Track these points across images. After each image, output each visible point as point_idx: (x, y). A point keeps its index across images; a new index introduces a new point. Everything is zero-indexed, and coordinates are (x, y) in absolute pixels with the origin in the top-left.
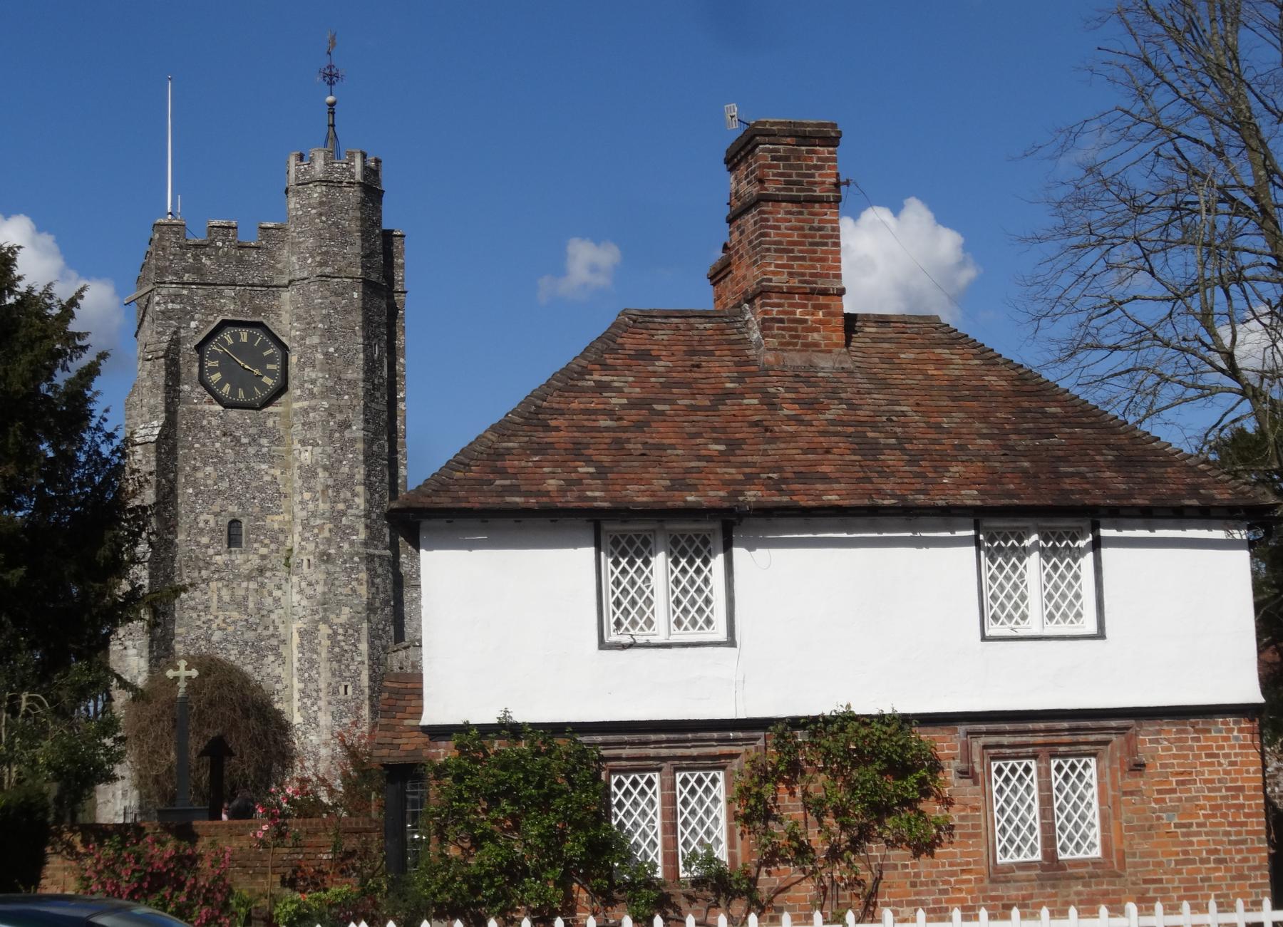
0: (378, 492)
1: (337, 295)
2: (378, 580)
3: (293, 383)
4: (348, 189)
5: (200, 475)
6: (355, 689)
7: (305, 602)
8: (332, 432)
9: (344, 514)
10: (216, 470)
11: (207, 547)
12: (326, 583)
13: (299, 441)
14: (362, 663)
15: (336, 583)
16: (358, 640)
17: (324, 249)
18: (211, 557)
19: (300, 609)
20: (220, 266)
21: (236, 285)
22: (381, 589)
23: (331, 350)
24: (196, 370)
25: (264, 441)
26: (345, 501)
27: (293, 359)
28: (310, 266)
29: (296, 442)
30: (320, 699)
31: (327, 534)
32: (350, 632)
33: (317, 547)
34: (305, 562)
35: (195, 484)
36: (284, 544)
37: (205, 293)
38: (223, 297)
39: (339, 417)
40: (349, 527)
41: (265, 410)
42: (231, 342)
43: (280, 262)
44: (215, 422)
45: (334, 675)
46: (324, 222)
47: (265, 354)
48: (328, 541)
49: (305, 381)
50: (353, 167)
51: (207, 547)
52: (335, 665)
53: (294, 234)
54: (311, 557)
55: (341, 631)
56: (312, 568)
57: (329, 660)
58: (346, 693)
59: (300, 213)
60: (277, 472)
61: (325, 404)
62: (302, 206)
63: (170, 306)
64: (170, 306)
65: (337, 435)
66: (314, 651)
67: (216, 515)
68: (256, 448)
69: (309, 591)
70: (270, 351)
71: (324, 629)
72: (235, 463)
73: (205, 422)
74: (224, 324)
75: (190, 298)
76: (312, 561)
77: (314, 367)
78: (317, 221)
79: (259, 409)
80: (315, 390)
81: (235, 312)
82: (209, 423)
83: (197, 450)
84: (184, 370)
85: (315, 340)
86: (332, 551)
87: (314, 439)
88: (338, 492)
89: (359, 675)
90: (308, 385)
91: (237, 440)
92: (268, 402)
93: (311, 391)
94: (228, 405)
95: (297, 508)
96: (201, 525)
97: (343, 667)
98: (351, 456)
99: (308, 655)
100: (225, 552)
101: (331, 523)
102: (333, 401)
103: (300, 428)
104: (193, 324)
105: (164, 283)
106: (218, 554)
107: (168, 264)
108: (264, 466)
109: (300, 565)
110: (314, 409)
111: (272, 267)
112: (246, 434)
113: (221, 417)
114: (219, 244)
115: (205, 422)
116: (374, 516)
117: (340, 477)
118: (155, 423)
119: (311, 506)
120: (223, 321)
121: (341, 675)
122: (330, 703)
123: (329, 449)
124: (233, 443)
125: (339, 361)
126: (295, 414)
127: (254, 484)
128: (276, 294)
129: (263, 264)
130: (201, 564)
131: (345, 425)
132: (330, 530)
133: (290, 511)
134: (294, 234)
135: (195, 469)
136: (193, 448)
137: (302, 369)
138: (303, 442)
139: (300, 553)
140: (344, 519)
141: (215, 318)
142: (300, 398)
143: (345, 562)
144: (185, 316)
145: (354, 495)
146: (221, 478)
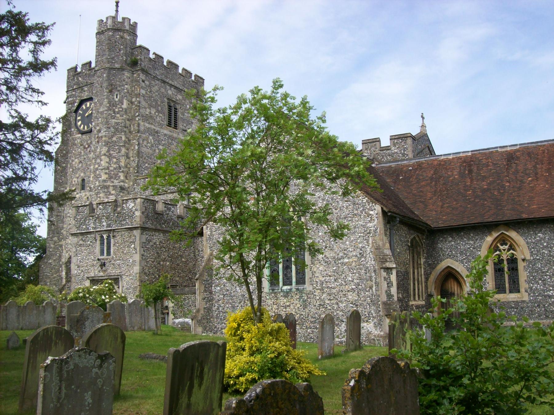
0: (115, 158)
5: (74, 163)
9: (97, 169)
48: (92, 182)
67: (78, 178)
116: (111, 168)
145: (101, 160)
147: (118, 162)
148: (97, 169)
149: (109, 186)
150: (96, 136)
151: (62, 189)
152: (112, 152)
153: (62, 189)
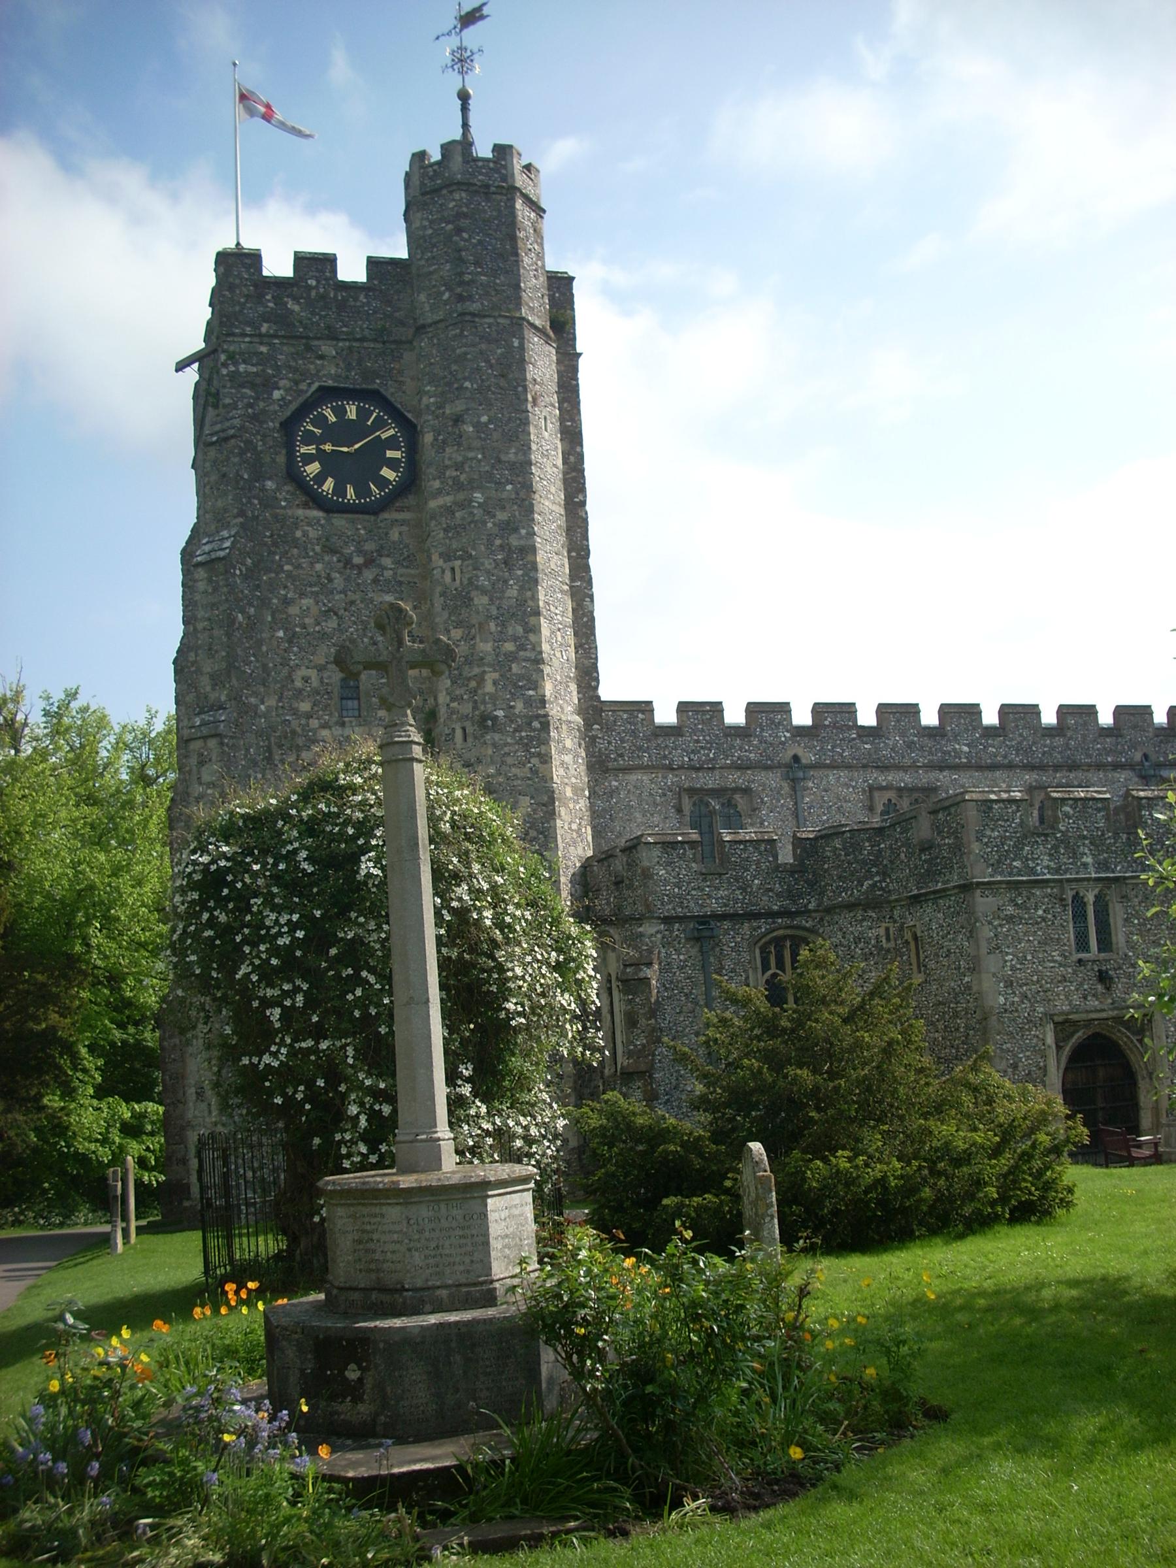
4: (499, 197)
5: (293, 610)
9: (512, 657)
10: (317, 603)
11: (309, 716)
13: (441, 555)
15: (509, 760)
17: (467, 277)
18: (315, 731)
20: (313, 313)
21: (338, 340)
24: (281, 459)
25: (387, 562)
26: (515, 639)
27: (428, 438)
28: (446, 303)
29: (435, 557)
33: (475, 708)
34: (459, 733)
35: (286, 625)
37: (292, 350)
39: (502, 516)
40: (521, 677)
41: (385, 515)
42: (332, 419)
44: (313, 534)
46: (466, 240)
48: (494, 698)
49: (447, 467)
50: (505, 167)
51: (309, 716)
53: (423, 262)
54: (468, 724)
56: (470, 740)
59: (430, 231)
62: (431, 222)
63: (242, 368)
68: (375, 571)
72: (344, 592)
73: (298, 534)
76: (469, 730)
77: (459, 445)
79: (375, 513)
80: (463, 477)
81: (336, 377)
82: (305, 534)
83: (289, 575)
84: (267, 459)
85: (459, 406)
86: (500, 713)
88: (503, 625)
91: (348, 562)
94: (329, 507)
96: (298, 684)
98: (520, 573)
100: (336, 723)
101: (495, 671)
103: (442, 535)
105: (233, 334)
106: (325, 726)
107: (237, 308)
112: (360, 552)
113: (322, 526)
114: (312, 282)
115: (298, 534)
118: (225, 533)
120: (321, 388)
126: (433, 517)
129: (375, 312)
130: (300, 741)
132: (495, 683)
134: (423, 262)
135: (286, 602)
138: (447, 557)
139: (449, 718)
141: (310, 385)
142: (439, 492)
148: (512, 657)
150: (498, 542)
151: (253, 700)
153: (253, 700)
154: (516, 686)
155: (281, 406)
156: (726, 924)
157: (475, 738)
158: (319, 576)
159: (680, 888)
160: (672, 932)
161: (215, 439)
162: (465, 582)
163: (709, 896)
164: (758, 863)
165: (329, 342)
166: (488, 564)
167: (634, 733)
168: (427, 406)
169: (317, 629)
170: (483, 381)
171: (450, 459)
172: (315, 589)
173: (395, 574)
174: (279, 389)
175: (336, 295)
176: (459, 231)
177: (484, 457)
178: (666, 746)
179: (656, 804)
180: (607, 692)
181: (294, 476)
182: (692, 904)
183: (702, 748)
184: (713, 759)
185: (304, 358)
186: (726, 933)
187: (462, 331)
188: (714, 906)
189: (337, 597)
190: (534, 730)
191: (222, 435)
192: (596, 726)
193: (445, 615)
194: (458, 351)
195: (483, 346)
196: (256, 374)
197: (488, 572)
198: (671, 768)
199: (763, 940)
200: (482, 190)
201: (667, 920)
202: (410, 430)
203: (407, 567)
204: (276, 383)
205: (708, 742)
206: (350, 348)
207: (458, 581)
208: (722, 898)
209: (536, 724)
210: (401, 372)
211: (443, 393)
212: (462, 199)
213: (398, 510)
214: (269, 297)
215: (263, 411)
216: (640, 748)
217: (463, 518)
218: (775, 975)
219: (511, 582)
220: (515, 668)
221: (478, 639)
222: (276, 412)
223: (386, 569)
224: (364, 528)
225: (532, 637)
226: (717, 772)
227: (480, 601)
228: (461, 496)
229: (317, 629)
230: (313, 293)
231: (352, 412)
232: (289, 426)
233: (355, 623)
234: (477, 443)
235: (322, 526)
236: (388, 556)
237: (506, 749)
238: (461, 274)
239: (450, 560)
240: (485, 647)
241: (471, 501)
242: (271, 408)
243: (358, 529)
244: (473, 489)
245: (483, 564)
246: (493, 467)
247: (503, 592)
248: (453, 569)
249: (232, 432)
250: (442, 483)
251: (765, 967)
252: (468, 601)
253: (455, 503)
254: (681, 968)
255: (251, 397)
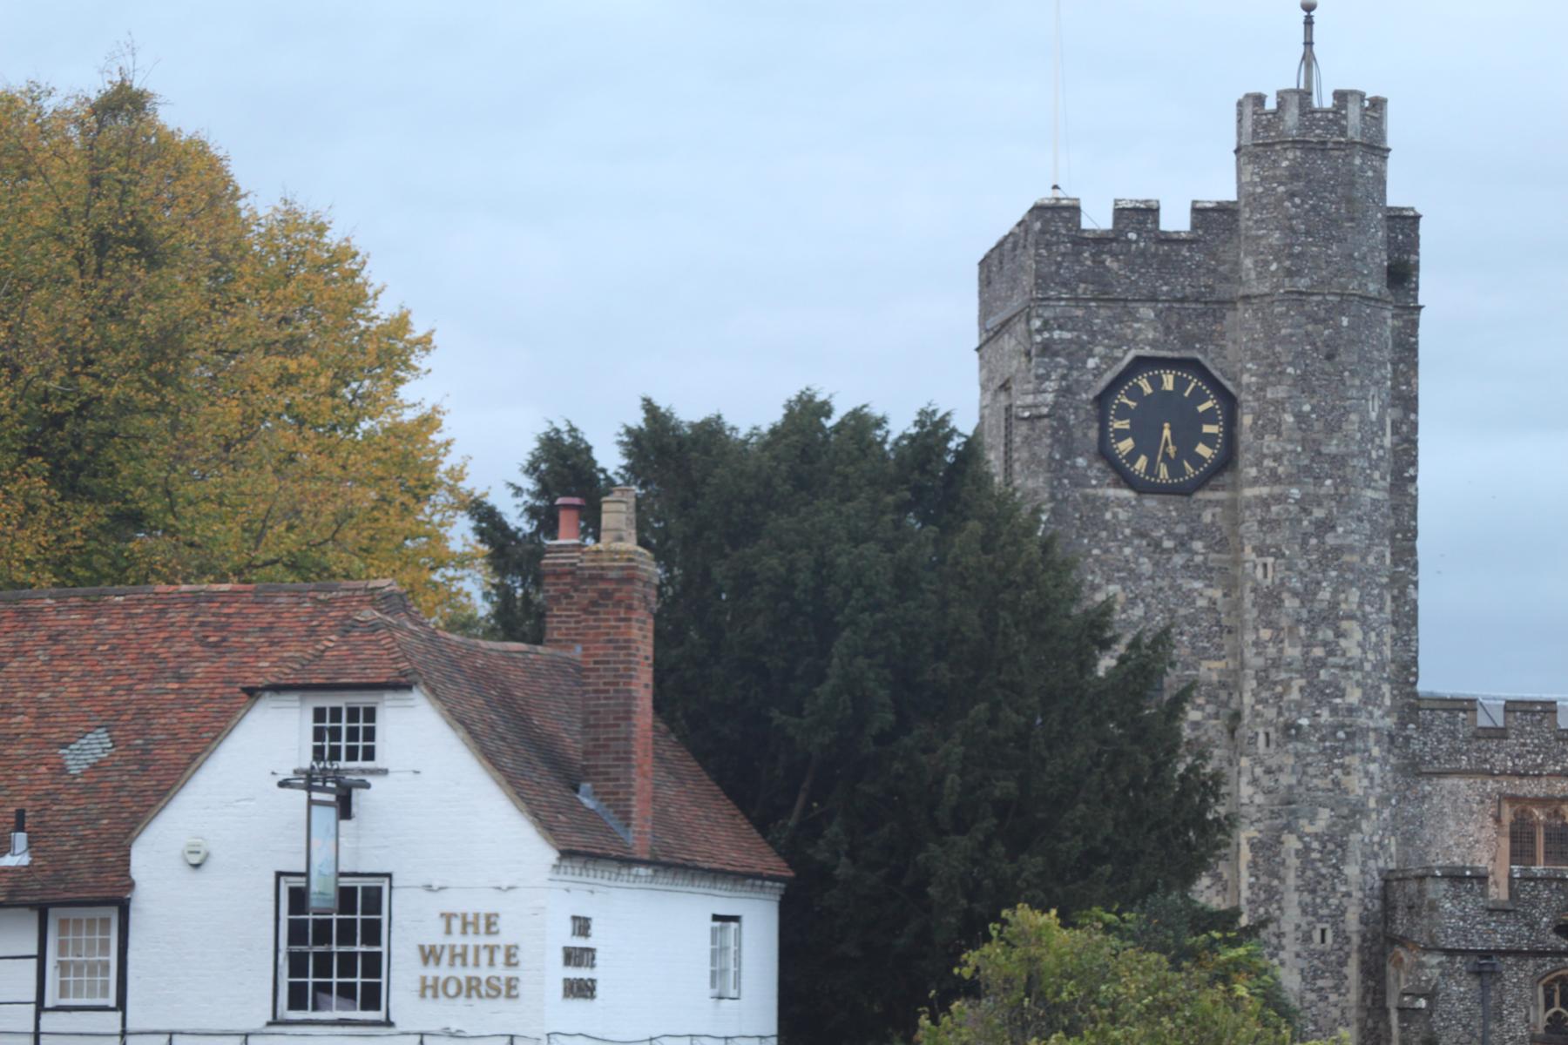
0: (1373, 630)
1: (1316, 322)
2: (1373, 767)
3: (1245, 457)
6: (1336, 935)
7: (1260, 799)
8: (1306, 537)
10: (1124, 589)
12: (1293, 772)
13: (1254, 549)
14: (1348, 895)
16: (1343, 860)
17: (1297, 249)
19: (1252, 809)
21: (1157, 301)
22: (1378, 781)
23: (1307, 408)
24: (1093, 434)
25: (1198, 545)
27: (1247, 420)
28: (1273, 274)
29: (1248, 549)
30: (1283, 948)
31: (1295, 695)
32: (1331, 846)
33: (1280, 714)
34: (1262, 738)
36: (1226, 704)
37: (1109, 313)
38: (1138, 320)
39: (1319, 513)
40: (1329, 684)
41: (1200, 495)
42: (1148, 390)
43: (1224, 262)
44: (1123, 515)
45: (1304, 912)
47: (1201, 408)
48: (1299, 706)
49: (1265, 456)
50: (1345, 117)
52: (1307, 898)
53: (1250, 223)
54: (1271, 730)
55: (1315, 845)
56: (1273, 746)
57: (1297, 889)
58: (1323, 941)
59: (1260, 190)
60: (1217, 594)
61: (1295, 492)
63: (1056, 334)
64: (1056, 334)
65: (1313, 541)
66: (1274, 874)
68: (1186, 556)
69: (1266, 782)
70: (1209, 404)
71: (1292, 843)
72: (1152, 578)
73: (1108, 516)
74: (1140, 364)
75: (1087, 322)
76: (1273, 736)
77: (1279, 434)
78: (1287, 204)
80: (1280, 470)
81: (1154, 344)
82: (1115, 515)
83: (1097, 559)
84: (1078, 434)
85: (1280, 392)
86: (1304, 722)
87: (1278, 547)
88: (1314, 630)
89: (1343, 913)
90: (1268, 463)
91: (1157, 545)
92: (1201, 483)
93: (1273, 471)
94: (1143, 487)
95: (1249, 653)
97: (1319, 900)
98: (1334, 574)
99: (1264, 880)
101: (1302, 677)
102: (1311, 489)
103: (1255, 527)
104: (1091, 363)
105: (1048, 299)
107: (1053, 268)
108: (1198, 585)
109: (1253, 740)
110: (1281, 499)
111: (1214, 271)
115: (1108, 516)
116: (1368, 667)
117: (1317, 606)
119: (1271, 651)
121: (1315, 914)
122: (1298, 955)
123: (1301, 564)
124: (1151, 549)
125: (1318, 426)
126: (1248, 507)
127: (1182, 611)
128: (1218, 314)
129: (1198, 267)
131: (1326, 526)
132: (1301, 689)
133: (1237, 654)
134: (1250, 223)
136: (1090, 555)
137: (1260, 436)
138: (1261, 551)
140: (1322, 672)
141: (1125, 353)
142: (1255, 482)
143: (1323, 739)
144: (1076, 353)
145: (1340, 634)
146: (1132, 602)
147: (1377, 648)
149: (1368, 729)
152: (1368, 608)
154: (1322, 692)
155: (1095, 376)
156: (1510, 960)
157: (1278, 745)
158: (1127, 561)
159: (1465, 921)
160: (1453, 964)
161: (1027, 414)
162: (1277, 581)
163: (1495, 931)
164: (1548, 900)
165: (1148, 304)
166: (1301, 564)
167: (1453, 735)
168: (1248, 385)
169: (1123, 616)
170: (1307, 365)
171: (1268, 447)
172: (1122, 574)
173: (1206, 559)
174: (1093, 356)
175: (1157, 249)
176: (1292, 195)
177: (1304, 449)
178: (1489, 749)
179: (1472, 813)
180: (1423, 687)
181: (1105, 453)
182: (1476, 938)
183: (1528, 752)
184: (1542, 765)
185: (1121, 322)
186: (1509, 968)
187: (1288, 310)
188: (1499, 941)
189: (1145, 584)
190: (1339, 740)
191: (1035, 411)
192: (1412, 726)
193: (1255, 613)
194: (1283, 331)
195: (1310, 327)
196: (1071, 341)
197: (1301, 573)
198: (1491, 774)
199: (1547, 979)
200: (1318, 146)
201: (1451, 953)
202: (1230, 403)
203: (1218, 552)
204: (1091, 350)
205: (1536, 746)
206: (1169, 309)
207: (1269, 581)
208: (1508, 933)
209: (1341, 734)
210: (1222, 335)
211: (1264, 375)
212: (1296, 157)
213: (1215, 489)
214: (1086, 255)
215: (1077, 381)
216: (1459, 751)
217: (1278, 514)
218: (1557, 1014)
219: (1324, 584)
220: (1323, 674)
221: (1286, 643)
222: (1089, 383)
223: (1197, 553)
224: (1176, 510)
225: (1343, 643)
226: (1544, 781)
227: (1290, 603)
228: (1277, 490)
229: (1123, 616)
230: (1134, 247)
231: (1168, 382)
232: (1102, 400)
233: (1162, 611)
234: (1298, 435)
235: (1133, 507)
236: (1199, 539)
237: (1309, 759)
238: (1292, 245)
239: (1262, 556)
240: (1293, 652)
241: (1287, 497)
242: (1085, 378)
243: (1169, 511)
244: (1291, 484)
245: (1296, 564)
246: (1312, 460)
247: (1315, 594)
248: (1265, 566)
249: (1045, 410)
250: (1259, 471)
251: (1549, 1003)
252: (1279, 603)
253: (1271, 496)
254: (1461, 1000)
255: (1064, 366)
